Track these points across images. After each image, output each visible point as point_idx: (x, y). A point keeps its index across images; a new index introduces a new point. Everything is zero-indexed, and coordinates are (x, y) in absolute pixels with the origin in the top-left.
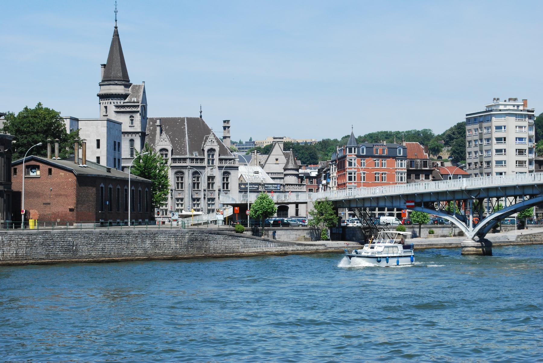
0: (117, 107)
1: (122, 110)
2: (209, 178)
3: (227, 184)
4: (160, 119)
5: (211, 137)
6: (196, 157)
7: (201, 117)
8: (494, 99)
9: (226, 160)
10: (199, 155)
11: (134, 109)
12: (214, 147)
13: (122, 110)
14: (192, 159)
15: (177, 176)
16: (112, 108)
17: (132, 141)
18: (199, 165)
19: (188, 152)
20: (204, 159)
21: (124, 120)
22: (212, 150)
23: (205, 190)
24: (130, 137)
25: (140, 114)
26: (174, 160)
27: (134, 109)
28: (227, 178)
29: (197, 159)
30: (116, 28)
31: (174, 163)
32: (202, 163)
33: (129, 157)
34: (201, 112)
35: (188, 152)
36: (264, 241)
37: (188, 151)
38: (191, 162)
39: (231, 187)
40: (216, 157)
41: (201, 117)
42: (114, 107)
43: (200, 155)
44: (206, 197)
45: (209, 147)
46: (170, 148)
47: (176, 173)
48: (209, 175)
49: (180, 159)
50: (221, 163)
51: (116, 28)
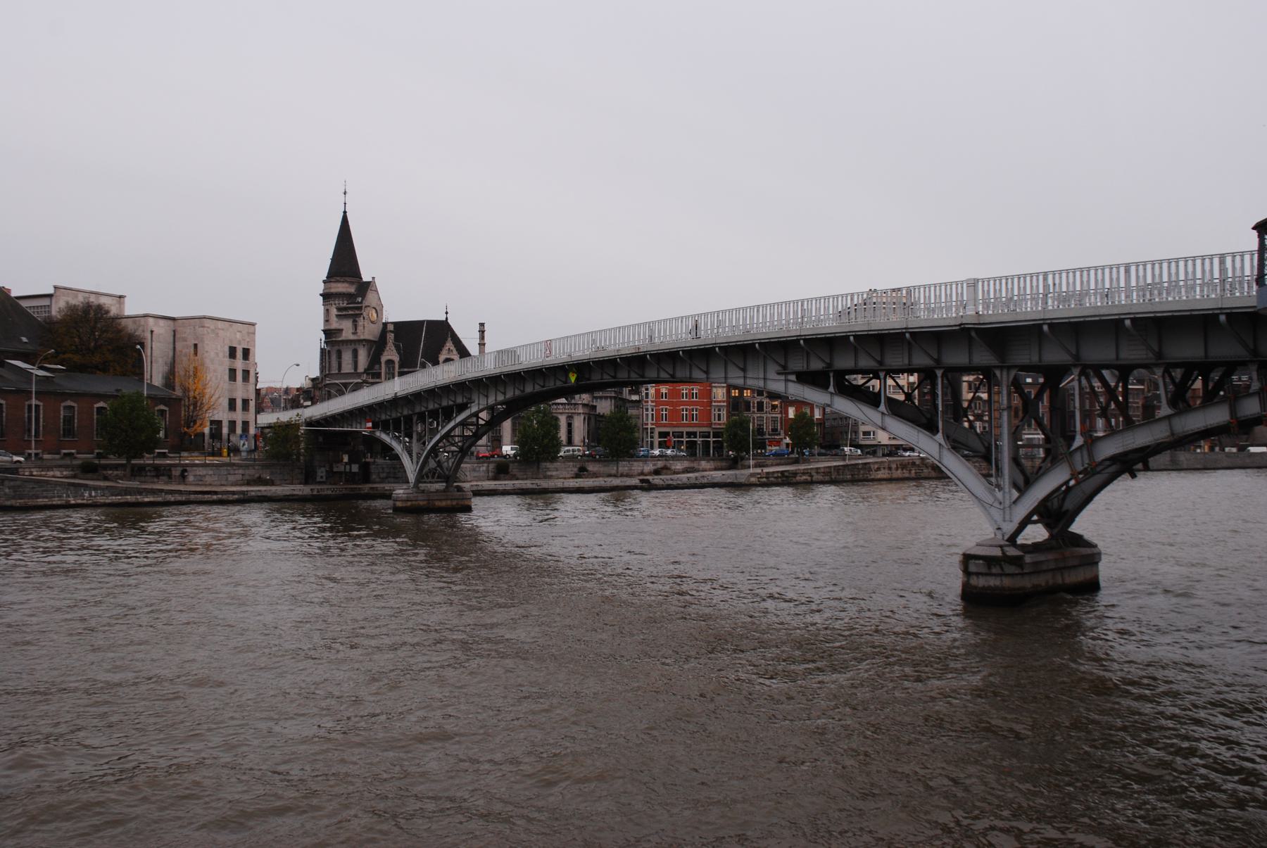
0: (339, 309)
1: (344, 313)
4: (392, 323)
5: (449, 344)
7: (447, 318)
11: (357, 312)
12: (452, 357)
13: (344, 313)
16: (334, 311)
21: (347, 325)
24: (353, 346)
25: (364, 318)
27: (357, 312)
30: (345, 212)
34: (447, 313)
36: (72, 488)
41: (447, 318)
42: (335, 310)
46: (396, 358)
51: (345, 212)
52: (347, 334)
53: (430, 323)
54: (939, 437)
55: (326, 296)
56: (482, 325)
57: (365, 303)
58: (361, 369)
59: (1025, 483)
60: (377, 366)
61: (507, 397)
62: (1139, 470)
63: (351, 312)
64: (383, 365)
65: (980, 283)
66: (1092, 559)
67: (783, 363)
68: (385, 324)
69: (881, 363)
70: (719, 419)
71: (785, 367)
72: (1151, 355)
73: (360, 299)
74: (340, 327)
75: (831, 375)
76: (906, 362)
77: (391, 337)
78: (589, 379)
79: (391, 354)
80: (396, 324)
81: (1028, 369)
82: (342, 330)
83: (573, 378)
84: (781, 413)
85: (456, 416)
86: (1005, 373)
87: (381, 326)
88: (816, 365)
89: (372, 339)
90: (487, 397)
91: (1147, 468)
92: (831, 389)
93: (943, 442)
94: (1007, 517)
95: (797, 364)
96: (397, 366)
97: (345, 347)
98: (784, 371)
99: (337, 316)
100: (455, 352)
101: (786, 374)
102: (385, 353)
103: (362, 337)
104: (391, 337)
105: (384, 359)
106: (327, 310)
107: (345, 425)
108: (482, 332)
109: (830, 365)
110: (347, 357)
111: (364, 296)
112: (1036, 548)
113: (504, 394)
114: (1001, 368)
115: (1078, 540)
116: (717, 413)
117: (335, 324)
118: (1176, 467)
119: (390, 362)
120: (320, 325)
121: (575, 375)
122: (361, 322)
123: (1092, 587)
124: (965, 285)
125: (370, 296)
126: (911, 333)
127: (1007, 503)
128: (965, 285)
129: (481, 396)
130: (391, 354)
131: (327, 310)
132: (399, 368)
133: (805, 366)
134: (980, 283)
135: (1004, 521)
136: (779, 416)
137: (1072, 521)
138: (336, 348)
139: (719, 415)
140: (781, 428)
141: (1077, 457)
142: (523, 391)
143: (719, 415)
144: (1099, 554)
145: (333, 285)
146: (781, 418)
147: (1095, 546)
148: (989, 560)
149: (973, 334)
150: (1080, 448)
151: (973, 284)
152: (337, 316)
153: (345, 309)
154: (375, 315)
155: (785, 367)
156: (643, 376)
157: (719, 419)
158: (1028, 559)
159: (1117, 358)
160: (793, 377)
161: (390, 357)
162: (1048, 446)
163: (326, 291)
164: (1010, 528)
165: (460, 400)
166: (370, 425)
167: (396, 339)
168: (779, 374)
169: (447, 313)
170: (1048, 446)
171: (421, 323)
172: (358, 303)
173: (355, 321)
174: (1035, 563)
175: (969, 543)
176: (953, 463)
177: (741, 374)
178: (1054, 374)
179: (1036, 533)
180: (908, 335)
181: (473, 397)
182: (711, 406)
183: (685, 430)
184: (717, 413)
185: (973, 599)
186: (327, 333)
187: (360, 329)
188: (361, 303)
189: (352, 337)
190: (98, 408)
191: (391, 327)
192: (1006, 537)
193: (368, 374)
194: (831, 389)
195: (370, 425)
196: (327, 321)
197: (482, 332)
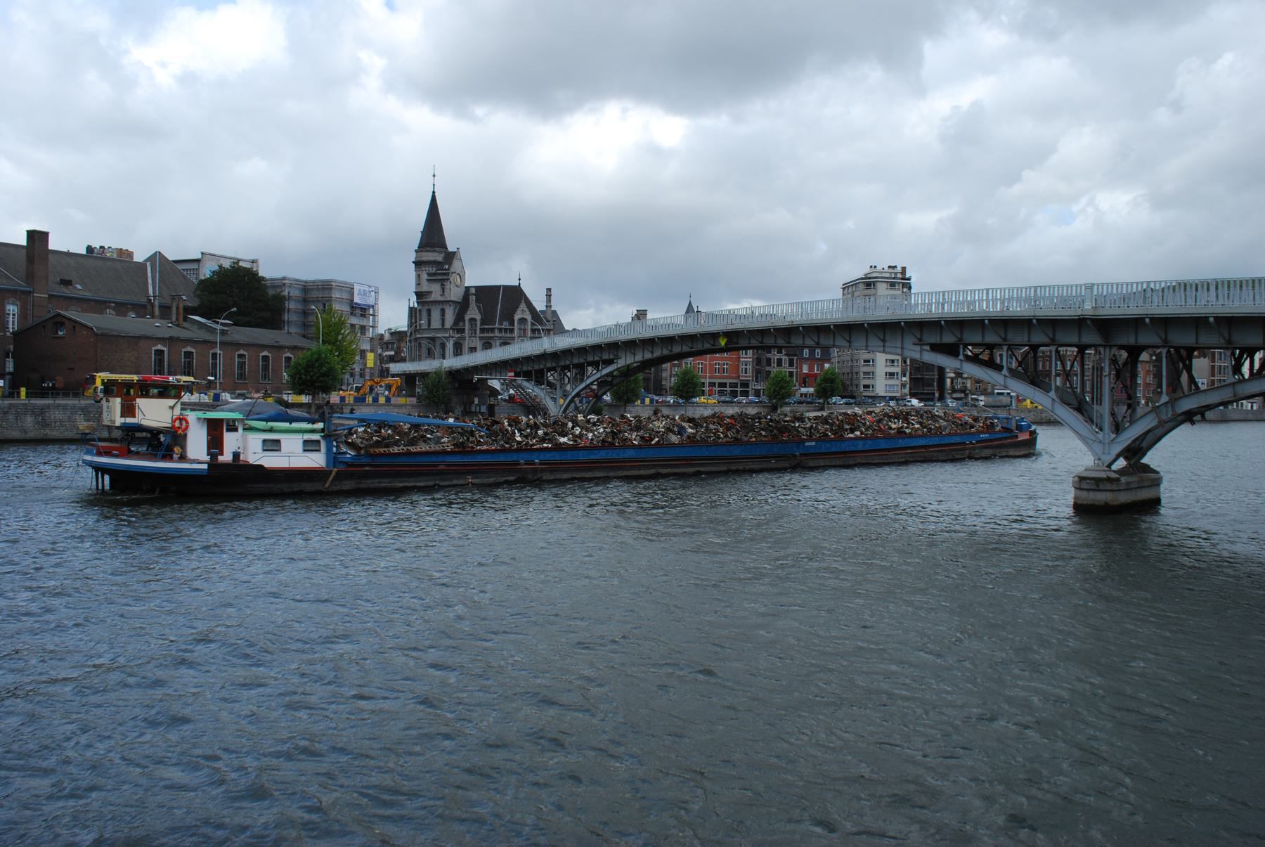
0: (429, 275)
5: (523, 306)
8: (871, 267)
12: (525, 317)
14: (500, 330)
16: (425, 276)
17: (443, 311)
18: (508, 335)
21: (436, 288)
22: (523, 320)
24: (441, 307)
26: (482, 330)
29: (506, 330)
30: (434, 192)
34: (520, 279)
40: (529, 327)
43: (510, 325)
45: (520, 316)
46: (478, 317)
47: (484, 344)
51: (434, 192)
52: (436, 295)
53: (506, 287)
54: (1052, 394)
55: (418, 264)
56: (549, 290)
57: (452, 270)
58: (448, 325)
59: (1118, 428)
60: (461, 324)
61: (655, 355)
62: (1198, 421)
63: (439, 278)
64: (467, 323)
65: (1096, 287)
66: (1157, 482)
67: (919, 337)
68: (468, 288)
69: (1005, 339)
70: (746, 373)
71: (920, 340)
72: (1223, 341)
73: (447, 267)
74: (430, 290)
75: (961, 346)
76: (1026, 339)
77: (473, 298)
78: (737, 344)
79: (473, 313)
80: (477, 288)
81: (1121, 347)
82: (431, 292)
83: (723, 342)
84: (797, 368)
85: (603, 368)
86: (1107, 350)
87: (464, 289)
88: (949, 339)
89: (456, 300)
90: (634, 354)
91: (1204, 419)
92: (961, 357)
93: (1055, 398)
94: (1106, 451)
95: (934, 339)
96: (479, 323)
97: (433, 307)
98: (920, 342)
99: (428, 280)
100: (528, 312)
101: (921, 345)
102: (469, 313)
103: (448, 299)
104: (473, 298)
105: (467, 317)
106: (419, 275)
107: (498, 374)
108: (549, 296)
109: (960, 340)
110: (436, 314)
111: (450, 264)
112: (1121, 472)
113: (652, 353)
114: (1105, 346)
115: (1147, 468)
116: (744, 367)
117: (425, 287)
118: (1224, 420)
119: (473, 320)
120: (412, 287)
121: (725, 340)
122: (447, 285)
123: (1155, 503)
124: (1083, 288)
125: (456, 264)
126: (1037, 320)
127: (1107, 441)
128: (1083, 288)
129: (628, 353)
130: (473, 313)
131: (419, 275)
132: (481, 324)
133: (939, 340)
134: (1096, 287)
135: (1104, 453)
136: (795, 370)
137: (1144, 454)
138: (426, 307)
139: (746, 369)
140: (797, 381)
141: (1163, 409)
142: (671, 351)
143: (746, 369)
144: (1161, 478)
145: (424, 254)
146: (797, 372)
147: (1158, 473)
148: (1098, 481)
149: (1089, 322)
150: (1166, 403)
151: (1090, 287)
152: (428, 280)
153: (434, 274)
154: (459, 280)
155: (920, 340)
156: (789, 343)
157: (746, 373)
158: (1123, 479)
159: (1197, 343)
160: (928, 348)
161: (472, 316)
162: (1129, 402)
163: (418, 259)
164: (1109, 458)
165: (606, 356)
166: (512, 374)
167: (477, 301)
168: (915, 344)
169: (520, 279)
170: (1129, 402)
171: (498, 287)
172: (446, 270)
173: (442, 285)
174: (1128, 483)
175: (1080, 470)
176: (1063, 412)
177: (882, 344)
178: (1134, 351)
179: (1121, 463)
180: (1034, 321)
181: (620, 354)
182: (739, 361)
183: (717, 381)
184: (744, 367)
185: (1080, 509)
186: (419, 295)
187: (447, 291)
188: (448, 269)
189: (440, 299)
190: (263, 356)
191: (473, 291)
192: (1106, 465)
194: (961, 357)
195: (512, 374)
196: (418, 284)
197: (549, 296)
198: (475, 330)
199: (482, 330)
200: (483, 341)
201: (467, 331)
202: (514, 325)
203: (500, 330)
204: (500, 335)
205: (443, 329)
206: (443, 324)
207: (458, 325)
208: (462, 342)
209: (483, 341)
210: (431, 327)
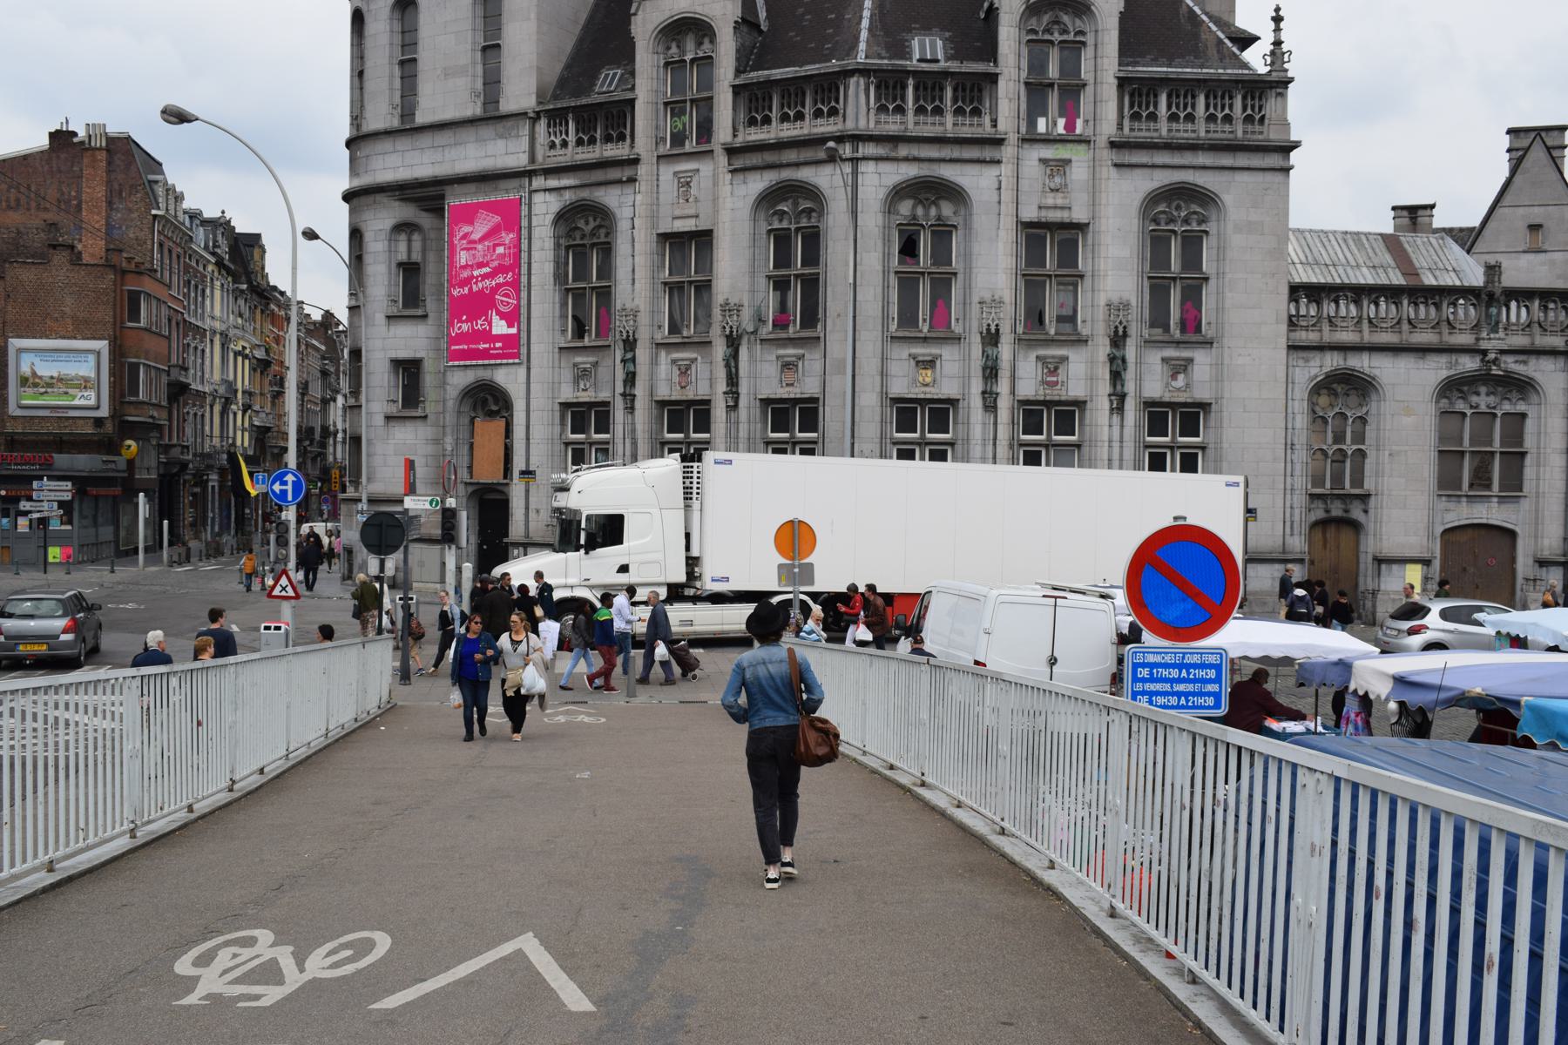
2: (1034, 234)
3: (1192, 295)
6: (925, 66)
9: (1183, 89)
10: (947, 59)
15: (776, 225)
19: (864, 35)
20: (993, 79)
23: (991, 338)
28: (1192, 244)
29: (930, 84)
31: (752, 122)
32: (976, 112)
33: (474, 109)
35: (864, 35)
37: (865, 23)
38: (882, 109)
39: (1220, 310)
44: (1003, 387)
48: (1030, 213)
49: (793, 91)
50: (1135, 117)
58: (520, 93)
64: (646, 59)
193: (557, 117)
198: (705, 105)
199: (753, 99)
200: (758, 184)
201: (644, 118)
202: (990, 51)
203: (889, 85)
204: (892, 125)
205: (491, 117)
206: (492, 83)
207: (587, 89)
208: (610, 198)
209: (758, 184)
210: (421, 118)
